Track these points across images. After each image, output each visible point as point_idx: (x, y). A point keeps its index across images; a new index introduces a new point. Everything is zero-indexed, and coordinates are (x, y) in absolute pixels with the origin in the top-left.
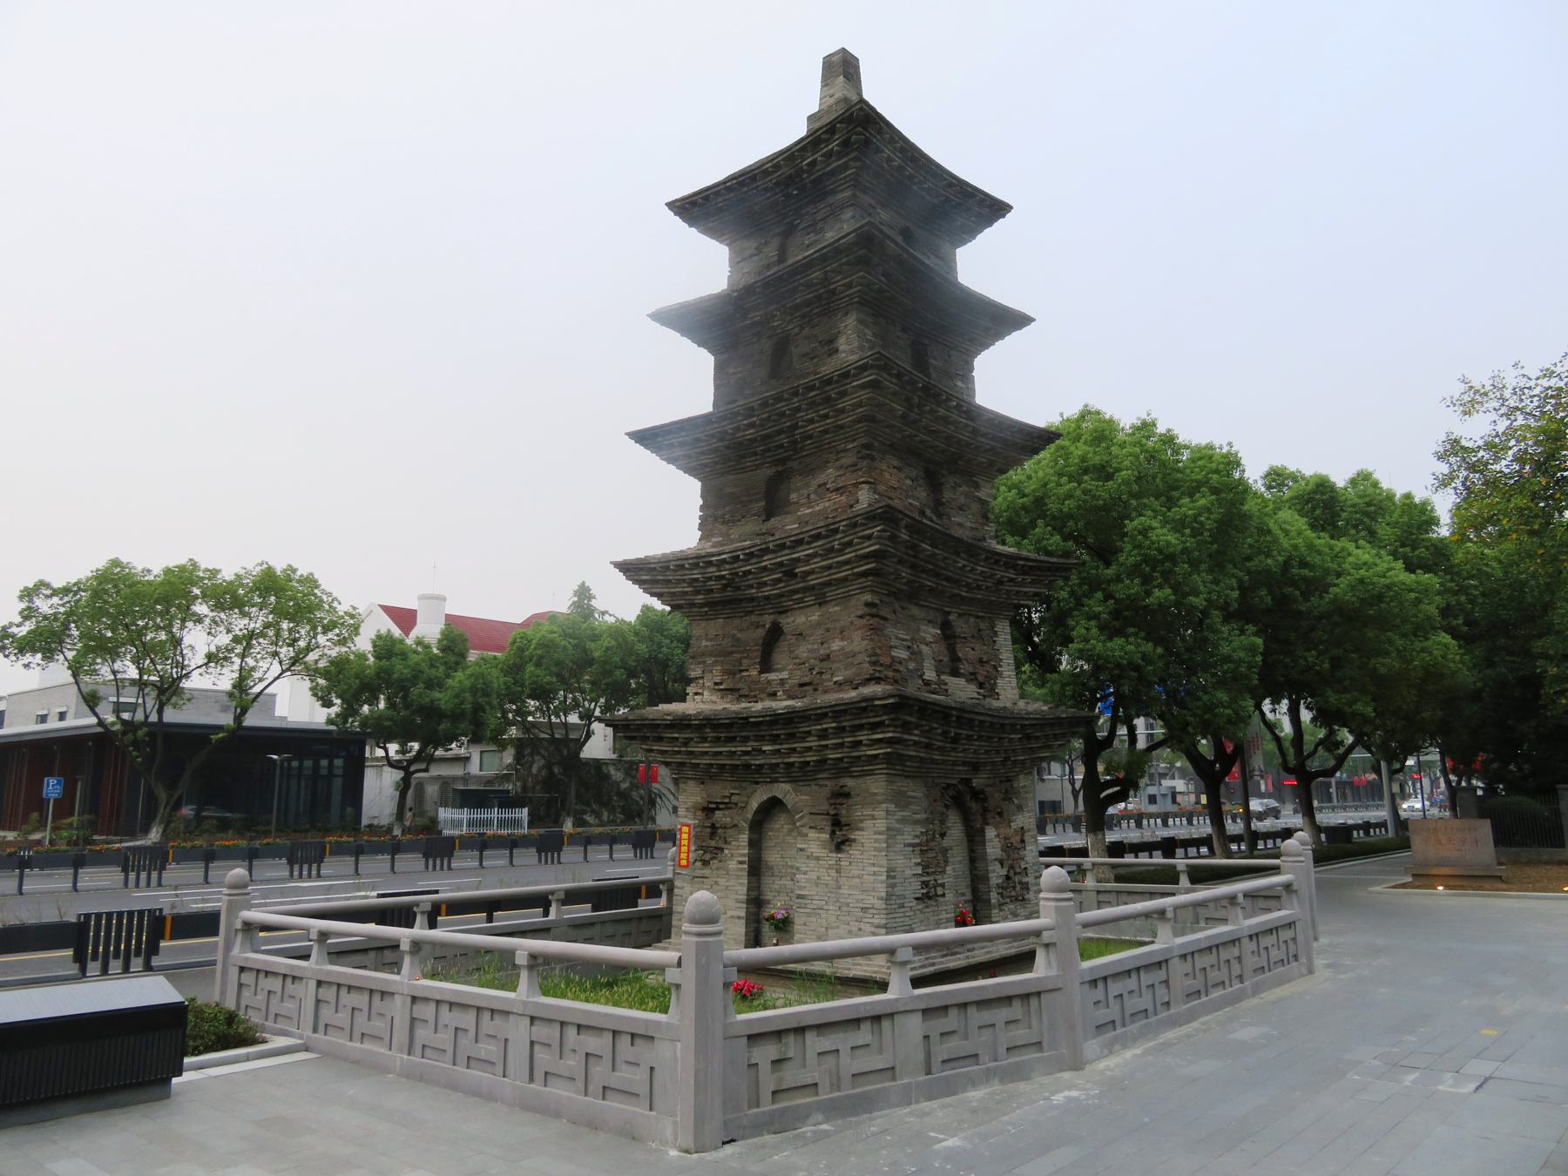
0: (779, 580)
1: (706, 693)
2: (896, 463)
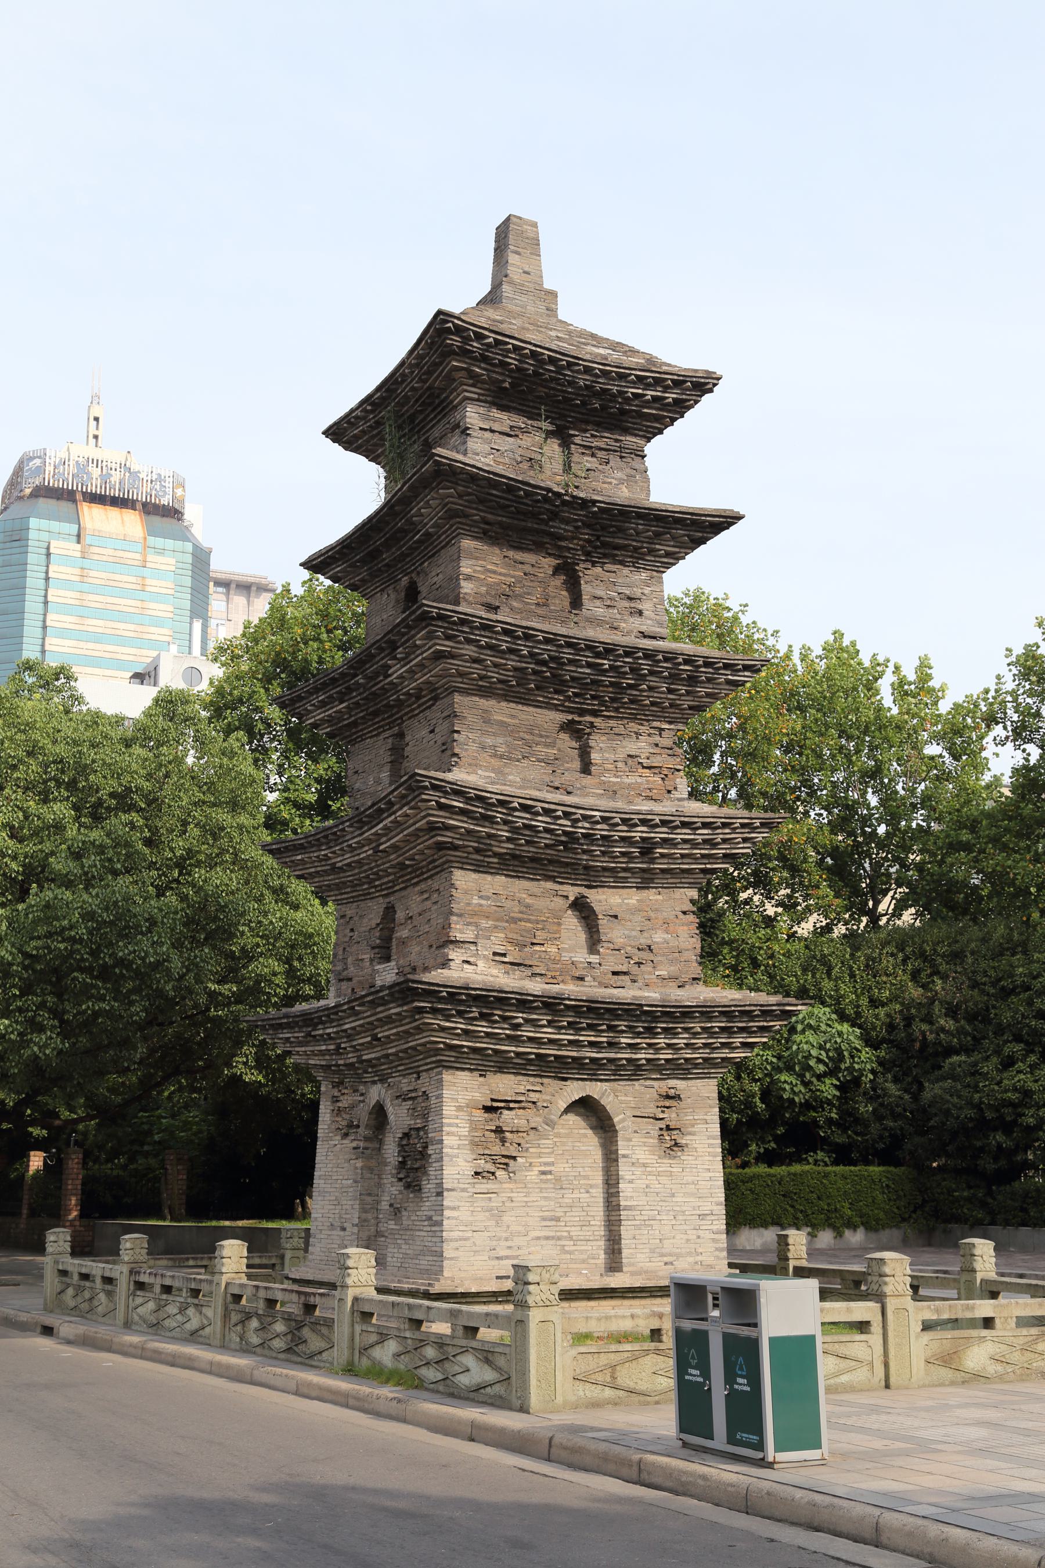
1: (481, 964)
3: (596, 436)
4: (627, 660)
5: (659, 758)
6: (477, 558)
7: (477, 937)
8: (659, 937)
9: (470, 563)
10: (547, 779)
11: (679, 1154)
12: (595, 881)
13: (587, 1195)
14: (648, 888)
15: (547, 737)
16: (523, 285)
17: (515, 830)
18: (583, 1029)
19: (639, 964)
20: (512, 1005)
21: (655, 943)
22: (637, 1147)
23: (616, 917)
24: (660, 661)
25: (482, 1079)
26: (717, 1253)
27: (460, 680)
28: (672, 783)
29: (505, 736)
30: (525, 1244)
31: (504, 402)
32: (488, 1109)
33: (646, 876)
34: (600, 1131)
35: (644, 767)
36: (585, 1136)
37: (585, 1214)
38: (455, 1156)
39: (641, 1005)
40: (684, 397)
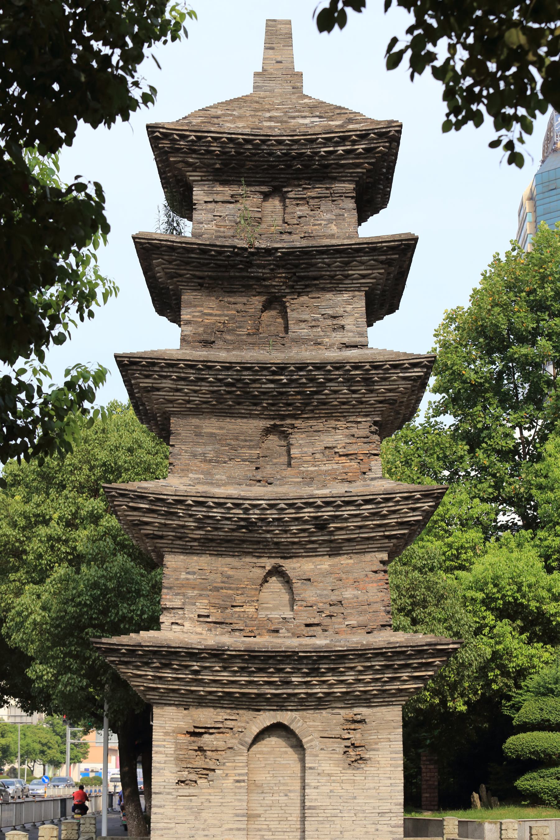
1: (187, 624)
3: (309, 188)
4: (301, 373)
5: (354, 446)
6: (195, 306)
7: (184, 604)
8: (348, 594)
9: (190, 310)
10: (250, 474)
11: (363, 766)
12: (288, 553)
13: (286, 798)
14: (340, 555)
15: (251, 441)
16: (272, 74)
17: (198, 520)
18: (253, 672)
19: (331, 616)
20: (183, 656)
21: (345, 598)
22: (325, 761)
23: (309, 580)
24: (330, 371)
25: (186, 712)
27: (171, 405)
28: (367, 466)
29: (214, 444)
30: (220, 833)
31: (224, 178)
32: (193, 734)
33: (332, 545)
34: (300, 749)
35: (340, 456)
36: (286, 753)
37: (283, 812)
38: (162, 769)
39: (298, 652)
40: (372, 145)
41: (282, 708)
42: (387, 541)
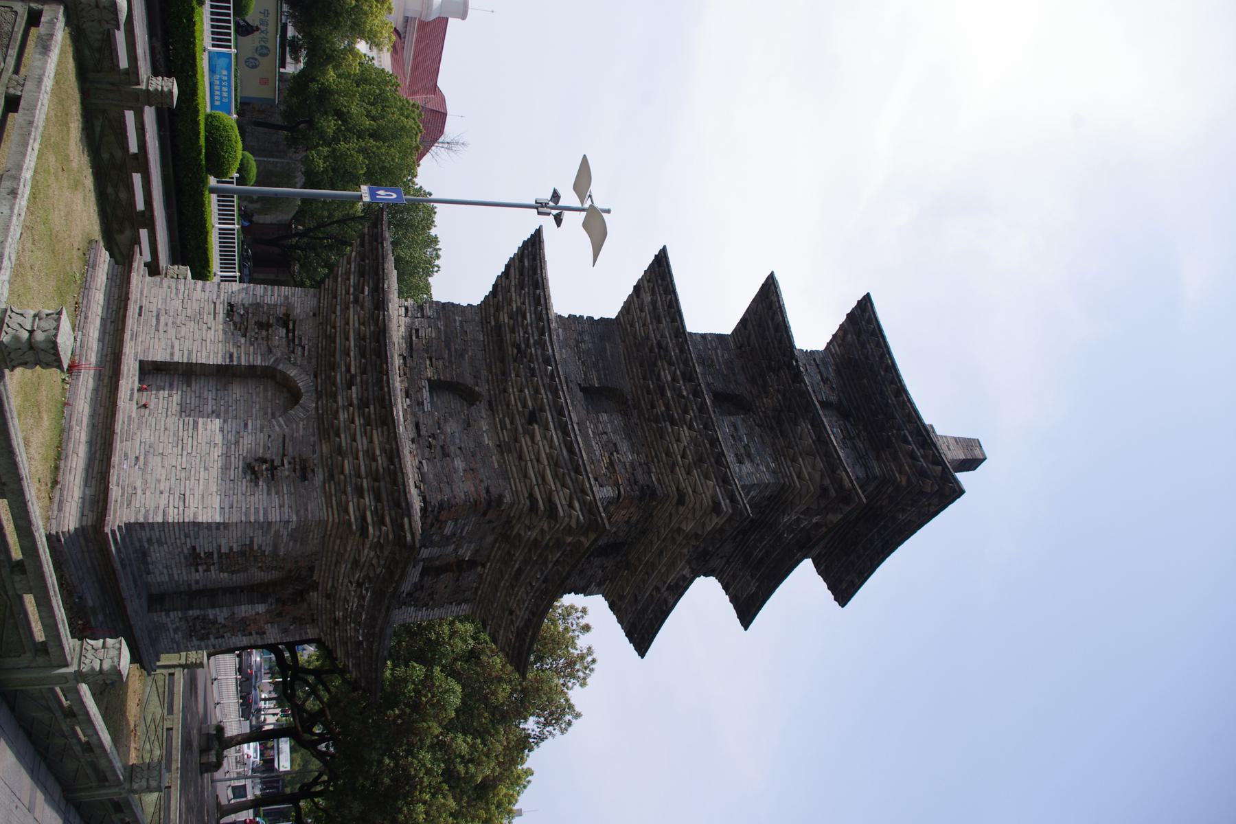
0: (525, 405)
2: (634, 519)
10: (573, 378)
19: (430, 447)
23: (469, 425)
26: (143, 511)
41: (319, 395)
42: (526, 495)
